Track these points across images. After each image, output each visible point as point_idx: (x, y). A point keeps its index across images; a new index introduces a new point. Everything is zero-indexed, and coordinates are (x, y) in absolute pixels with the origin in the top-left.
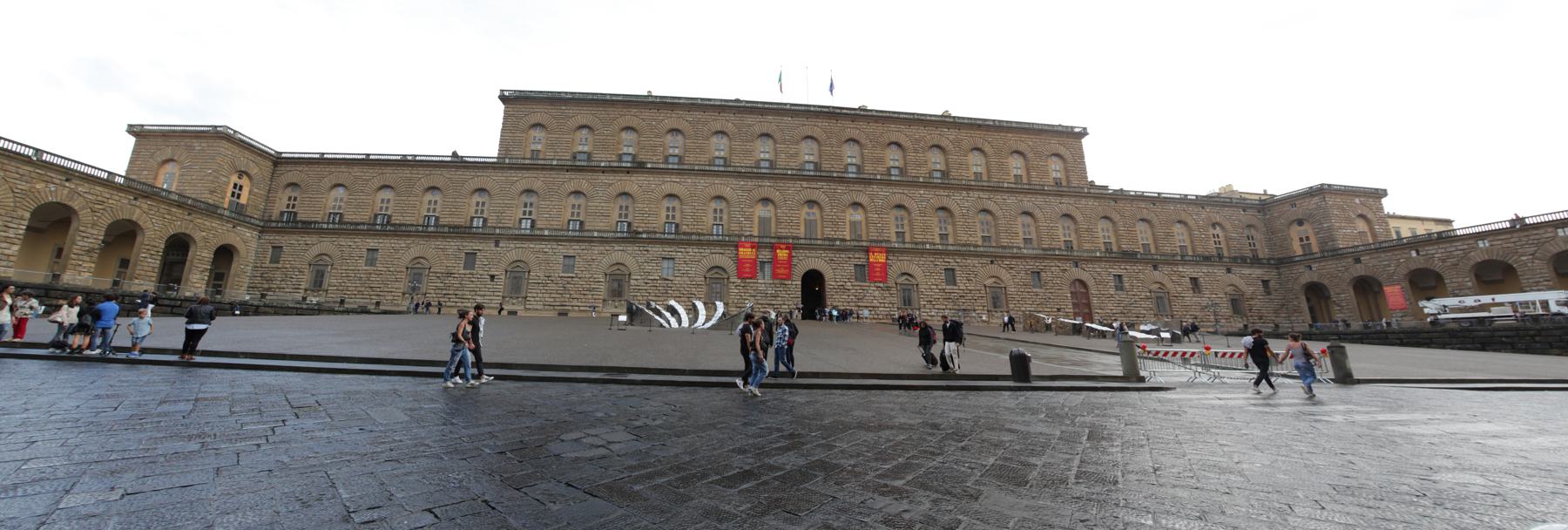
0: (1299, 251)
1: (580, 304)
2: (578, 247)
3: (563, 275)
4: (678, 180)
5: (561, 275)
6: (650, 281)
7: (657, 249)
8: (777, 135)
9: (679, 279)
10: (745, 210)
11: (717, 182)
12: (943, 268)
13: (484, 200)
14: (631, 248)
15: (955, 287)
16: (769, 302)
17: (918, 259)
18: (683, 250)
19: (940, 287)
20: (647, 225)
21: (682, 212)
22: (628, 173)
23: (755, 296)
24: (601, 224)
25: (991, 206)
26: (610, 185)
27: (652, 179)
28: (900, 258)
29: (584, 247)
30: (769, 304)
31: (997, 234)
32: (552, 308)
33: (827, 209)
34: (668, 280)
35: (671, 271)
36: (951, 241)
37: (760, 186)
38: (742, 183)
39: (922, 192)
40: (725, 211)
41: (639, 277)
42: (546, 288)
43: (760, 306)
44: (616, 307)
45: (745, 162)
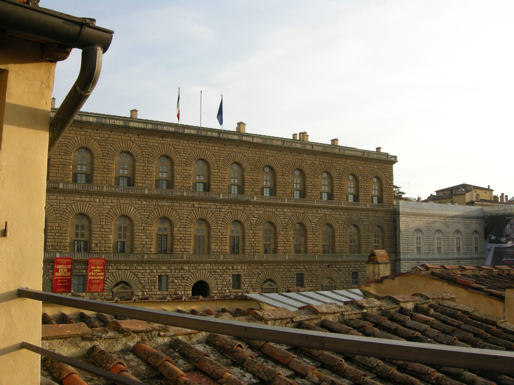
4: (87, 200)
12: (295, 273)
27: (62, 198)
33: (213, 227)
39: (286, 210)
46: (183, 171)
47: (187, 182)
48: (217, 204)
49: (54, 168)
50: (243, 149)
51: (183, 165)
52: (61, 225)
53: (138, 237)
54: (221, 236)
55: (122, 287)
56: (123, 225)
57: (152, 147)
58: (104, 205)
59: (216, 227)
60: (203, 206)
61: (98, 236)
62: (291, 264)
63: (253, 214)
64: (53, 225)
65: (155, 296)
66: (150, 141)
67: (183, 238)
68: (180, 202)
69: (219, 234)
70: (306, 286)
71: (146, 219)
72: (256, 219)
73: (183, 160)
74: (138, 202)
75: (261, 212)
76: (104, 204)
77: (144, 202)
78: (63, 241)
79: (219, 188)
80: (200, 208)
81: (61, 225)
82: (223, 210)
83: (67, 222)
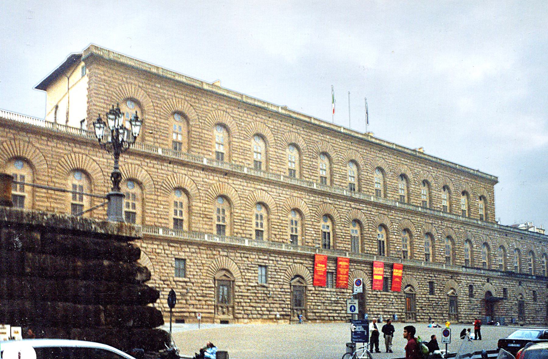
1: (196, 310)
2: (188, 250)
3: (178, 279)
4: (266, 188)
5: (176, 279)
6: (250, 288)
7: (254, 257)
8: (333, 155)
9: (271, 286)
10: (315, 223)
11: (295, 194)
13: (81, 184)
15: (434, 297)
16: (334, 308)
17: (415, 274)
18: (274, 258)
19: (427, 296)
20: (245, 232)
21: (268, 220)
22: (226, 175)
23: (324, 303)
24: (206, 227)
25: (451, 232)
28: (408, 273)
29: (194, 250)
30: (333, 310)
31: (454, 255)
35: (264, 278)
36: (431, 258)
37: (324, 203)
38: (312, 198)
39: (419, 219)
40: (299, 224)
41: (241, 284)
43: (328, 312)
44: (224, 313)
45: (313, 177)
46: (341, 170)
47: (344, 181)
48: (367, 206)
51: (340, 164)
52: (246, 212)
53: (309, 232)
54: (372, 238)
55: (299, 281)
56: (294, 219)
58: (280, 196)
59: (367, 229)
60: (357, 207)
61: (276, 227)
64: (240, 212)
65: (324, 293)
67: (343, 237)
69: (371, 236)
71: (314, 214)
72: (397, 225)
73: (340, 159)
74: (307, 197)
75: (401, 219)
76: (280, 195)
79: (368, 191)
83: (250, 210)
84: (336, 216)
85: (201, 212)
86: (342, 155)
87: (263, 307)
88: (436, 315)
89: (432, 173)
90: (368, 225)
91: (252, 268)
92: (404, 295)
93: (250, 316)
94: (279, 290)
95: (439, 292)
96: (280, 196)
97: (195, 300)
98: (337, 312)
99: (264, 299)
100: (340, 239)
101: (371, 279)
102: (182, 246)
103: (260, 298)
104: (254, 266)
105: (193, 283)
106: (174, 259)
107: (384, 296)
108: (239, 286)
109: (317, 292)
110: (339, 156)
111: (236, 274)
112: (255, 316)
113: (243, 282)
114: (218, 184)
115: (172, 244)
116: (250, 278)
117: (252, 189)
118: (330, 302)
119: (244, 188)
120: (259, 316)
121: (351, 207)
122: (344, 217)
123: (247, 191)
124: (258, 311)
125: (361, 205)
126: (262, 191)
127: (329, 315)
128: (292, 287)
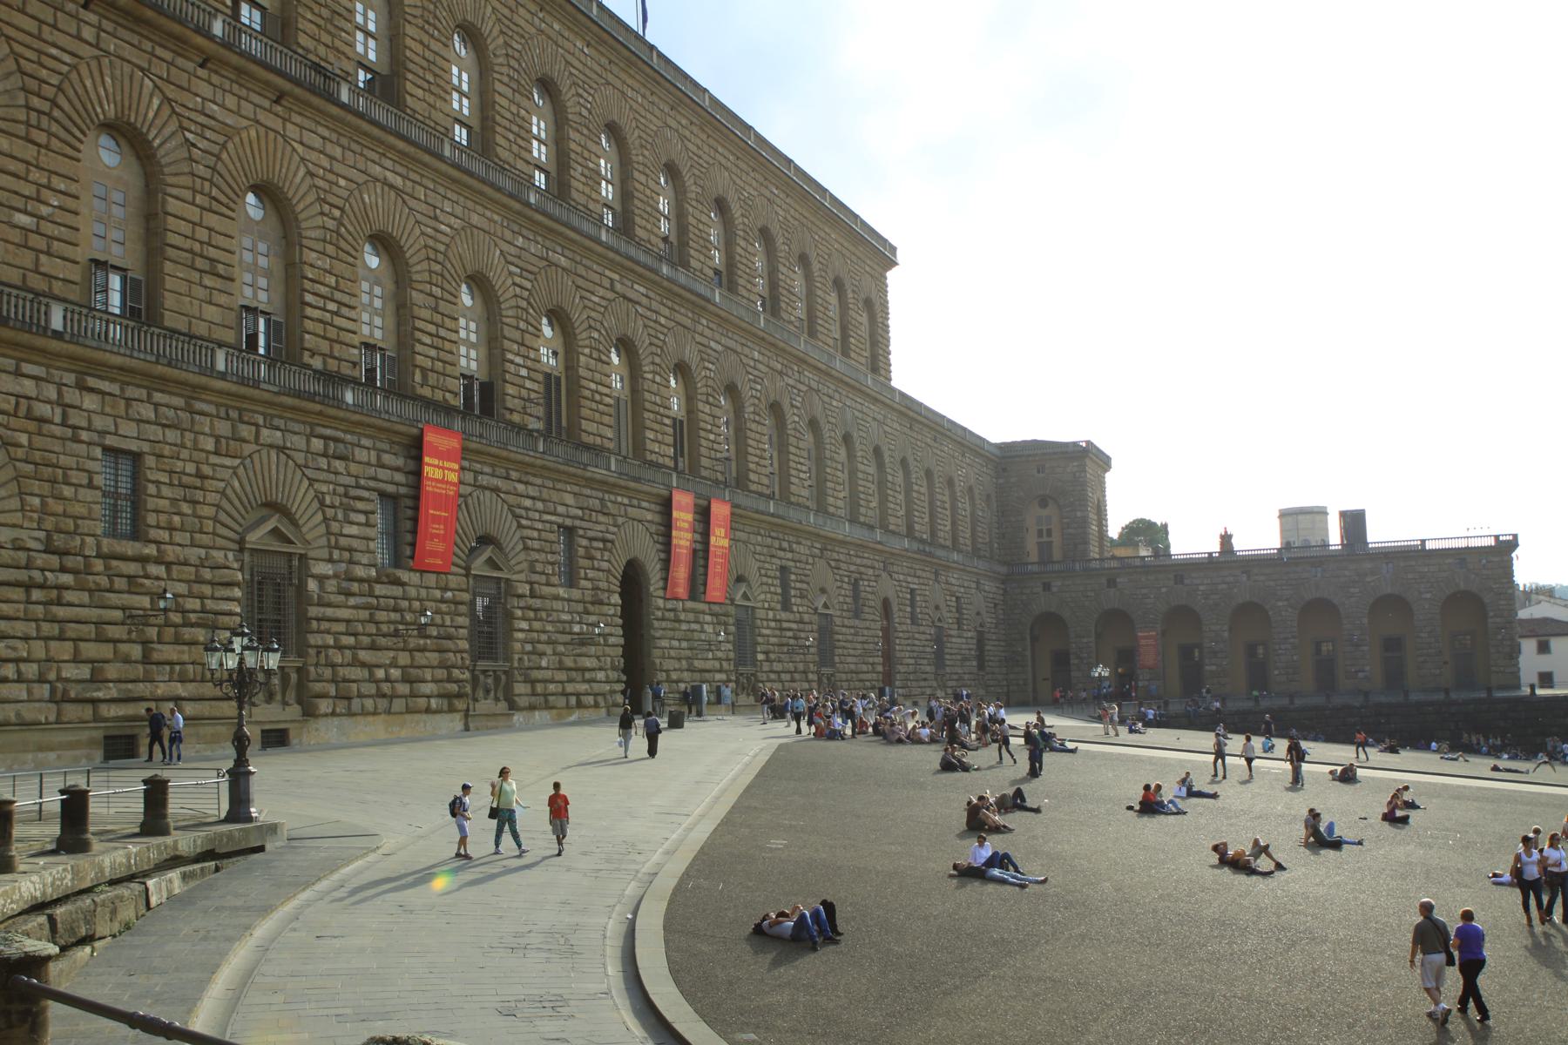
0: (1034, 557)
1: (180, 690)
2: (147, 412)
4: (398, 181)
5: (107, 544)
6: (355, 587)
11: (475, 219)
14: (299, 441)
15: (791, 617)
22: (277, 101)
26: (229, 133)
27: (338, 152)
32: (87, 711)
34: (397, 582)
37: (551, 264)
38: (520, 241)
42: (61, 612)
49: (309, 16)
50: (684, 122)
51: (585, 131)
57: (527, 36)
58: (436, 218)
62: (773, 534)
63: (709, 351)
66: (521, 10)
68: (588, 263)
70: (795, 609)
74: (508, 235)
75: (720, 348)
77: (521, 239)
78: (348, 337)
80: (625, 297)
81: (339, 267)
82: (663, 320)
84: (578, 316)
85: (197, 247)
86: (590, 99)
87: (394, 664)
88: (797, 676)
89: (778, 210)
90: (653, 363)
91: (360, 505)
92: (732, 610)
93: (356, 704)
94: (438, 594)
95: (799, 601)
96: (436, 218)
97: (178, 641)
98: (588, 675)
99: (396, 634)
100: (588, 403)
101: (663, 556)
102: (132, 392)
103: (384, 628)
104: (366, 494)
105: (168, 565)
106: (98, 452)
107: (691, 616)
108: (321, 579)
109: (537, 603)
110: (582, 101)
111: (312, 526)
112: (369, 703)
113: (330, 560)
114: (253, 133)
115: (92, 382)
116: (355, 543)
117: (353, 174)
118: (567, 638)
119: (338, 167)
120: (382, 704)
121: (612, 289)
122: (598, 326)
123: (342, 182)
124: (377, 682)
125: (636, 286)
126: (386, 188)
127: (570, 688)
128: (471, 581)
